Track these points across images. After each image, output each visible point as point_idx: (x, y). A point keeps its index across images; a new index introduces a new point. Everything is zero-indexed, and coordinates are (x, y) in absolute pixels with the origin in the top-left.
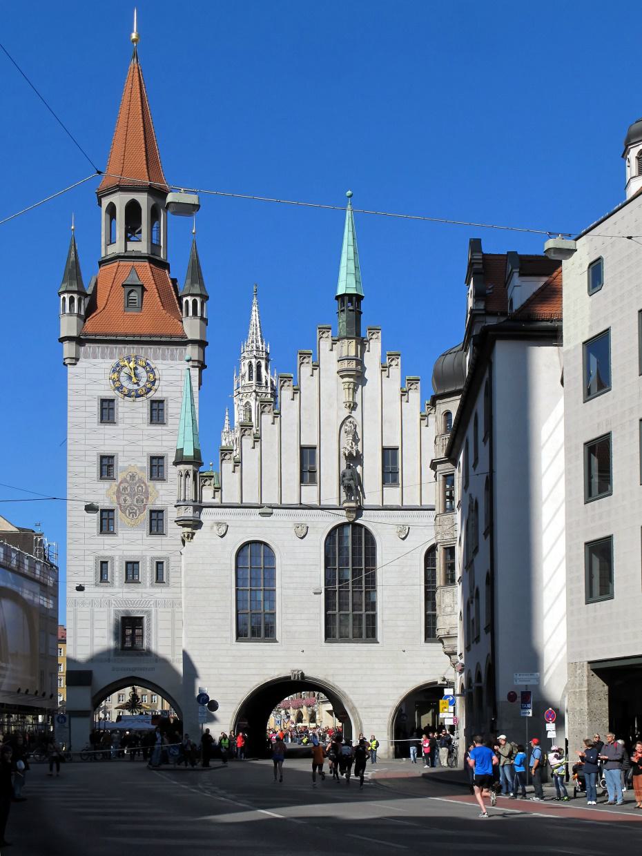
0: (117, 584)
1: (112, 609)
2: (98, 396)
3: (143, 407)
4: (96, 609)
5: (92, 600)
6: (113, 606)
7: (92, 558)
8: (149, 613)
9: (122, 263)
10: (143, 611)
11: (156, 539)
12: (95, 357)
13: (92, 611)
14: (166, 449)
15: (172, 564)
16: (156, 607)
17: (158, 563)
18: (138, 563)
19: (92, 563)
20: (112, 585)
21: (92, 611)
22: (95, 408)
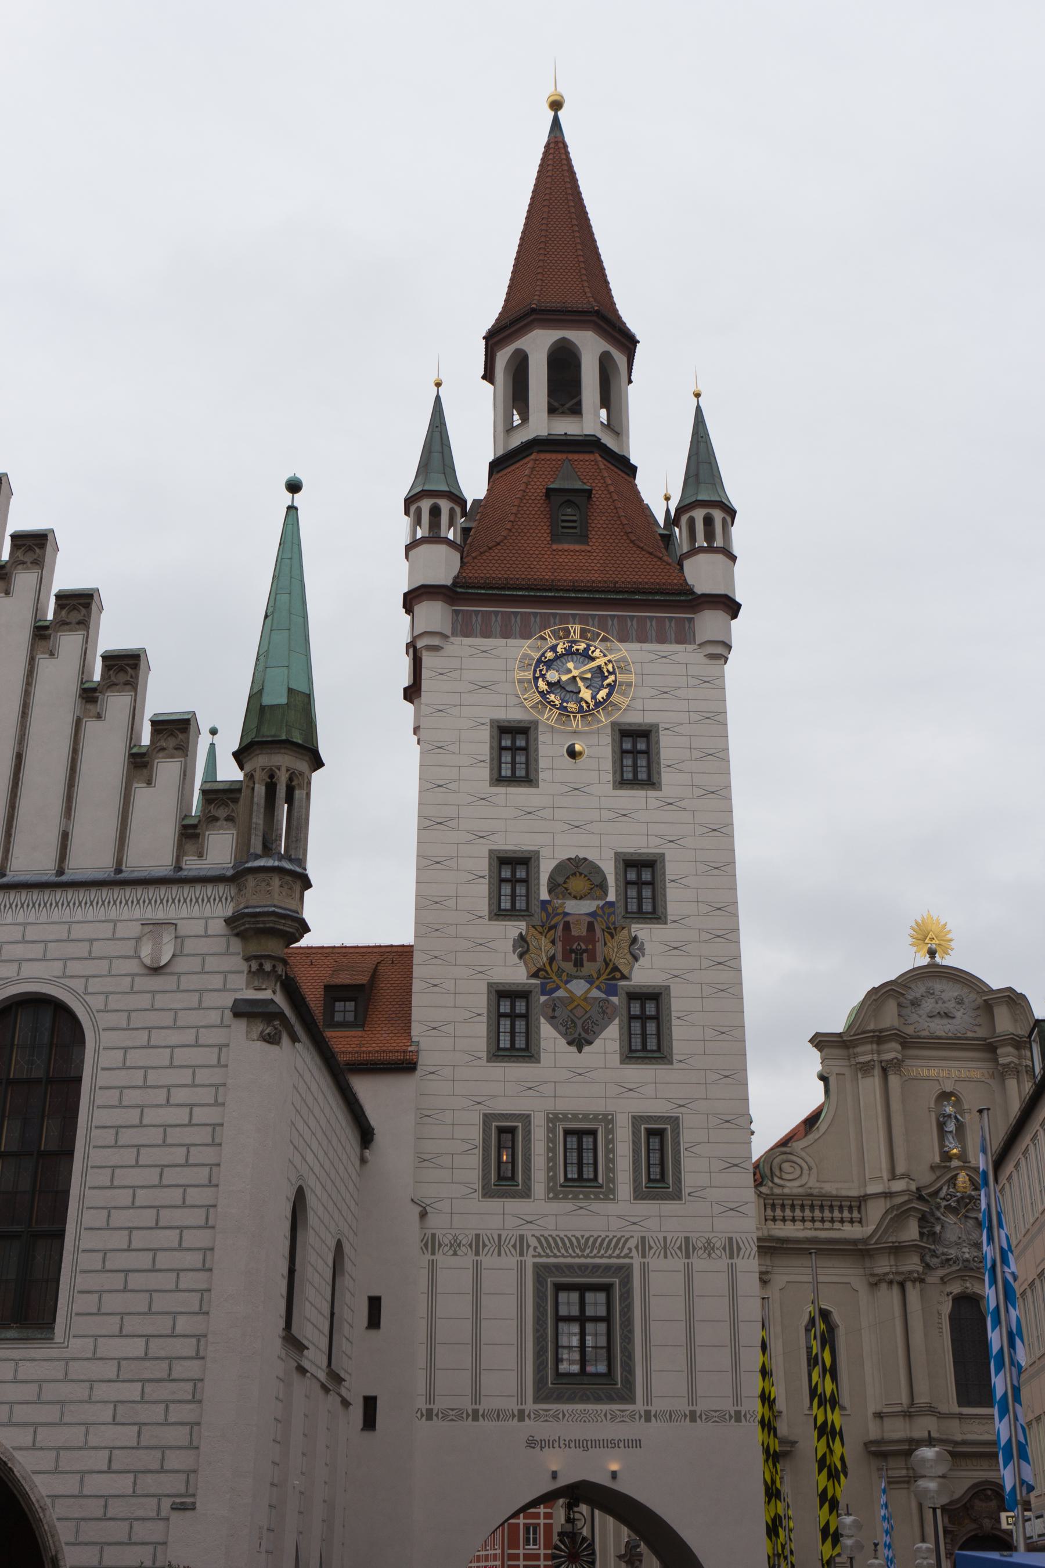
0: (539, 1187)
1: (530, 1261)
2: (492, 721)
3: (599, 750)
4: (488, 1260)
5: (477, 1236)
6: (531, 1251)
7: (476, 1119)
8: (624, 1272)
9: (543, 456)
10: (607, 1268)
11: (639, 1073)
12: (486, 634)
13: (477, 1266)
14: (654, 841)
15: (687, 1137)
16: (644, 1256)
17: (650, 1133)
18: (593, 1133)
19: (475, 1134)
20: (526, 1194)
21: (477, 1266)
22: (482, 743)
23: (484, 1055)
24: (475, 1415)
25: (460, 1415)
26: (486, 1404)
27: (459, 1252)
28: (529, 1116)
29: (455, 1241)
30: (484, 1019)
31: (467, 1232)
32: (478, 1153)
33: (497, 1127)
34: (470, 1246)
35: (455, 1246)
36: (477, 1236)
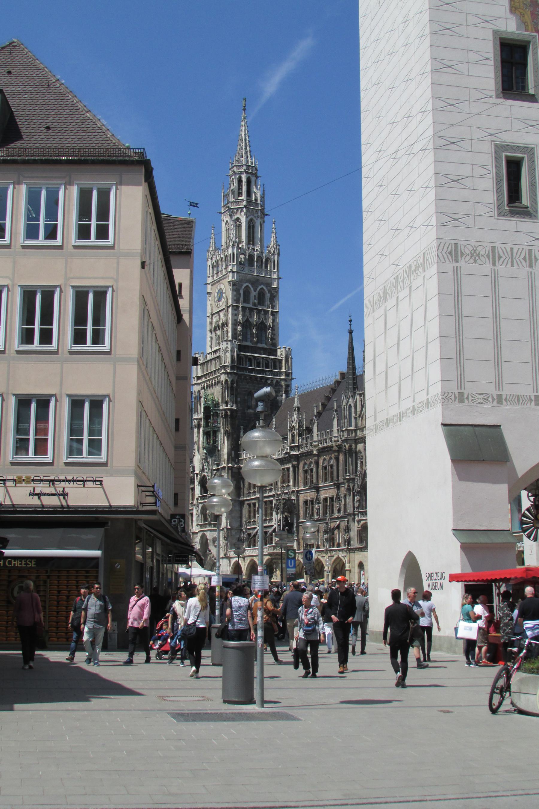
5: (493, 248)
7: (488, 148)
19: (488, 160)
23: (493, 93)
24: (500, 399)
25: (486, 399)
26: (506, 392)
27: (478, 261)
28: (532, 149)
29: (475, 251)
30: (492, 63)
31: (485, 244)
32: (492, 176)
33: (507, 157)
34: (488, 256)
35: (475, 256)
36: (493, 248)
